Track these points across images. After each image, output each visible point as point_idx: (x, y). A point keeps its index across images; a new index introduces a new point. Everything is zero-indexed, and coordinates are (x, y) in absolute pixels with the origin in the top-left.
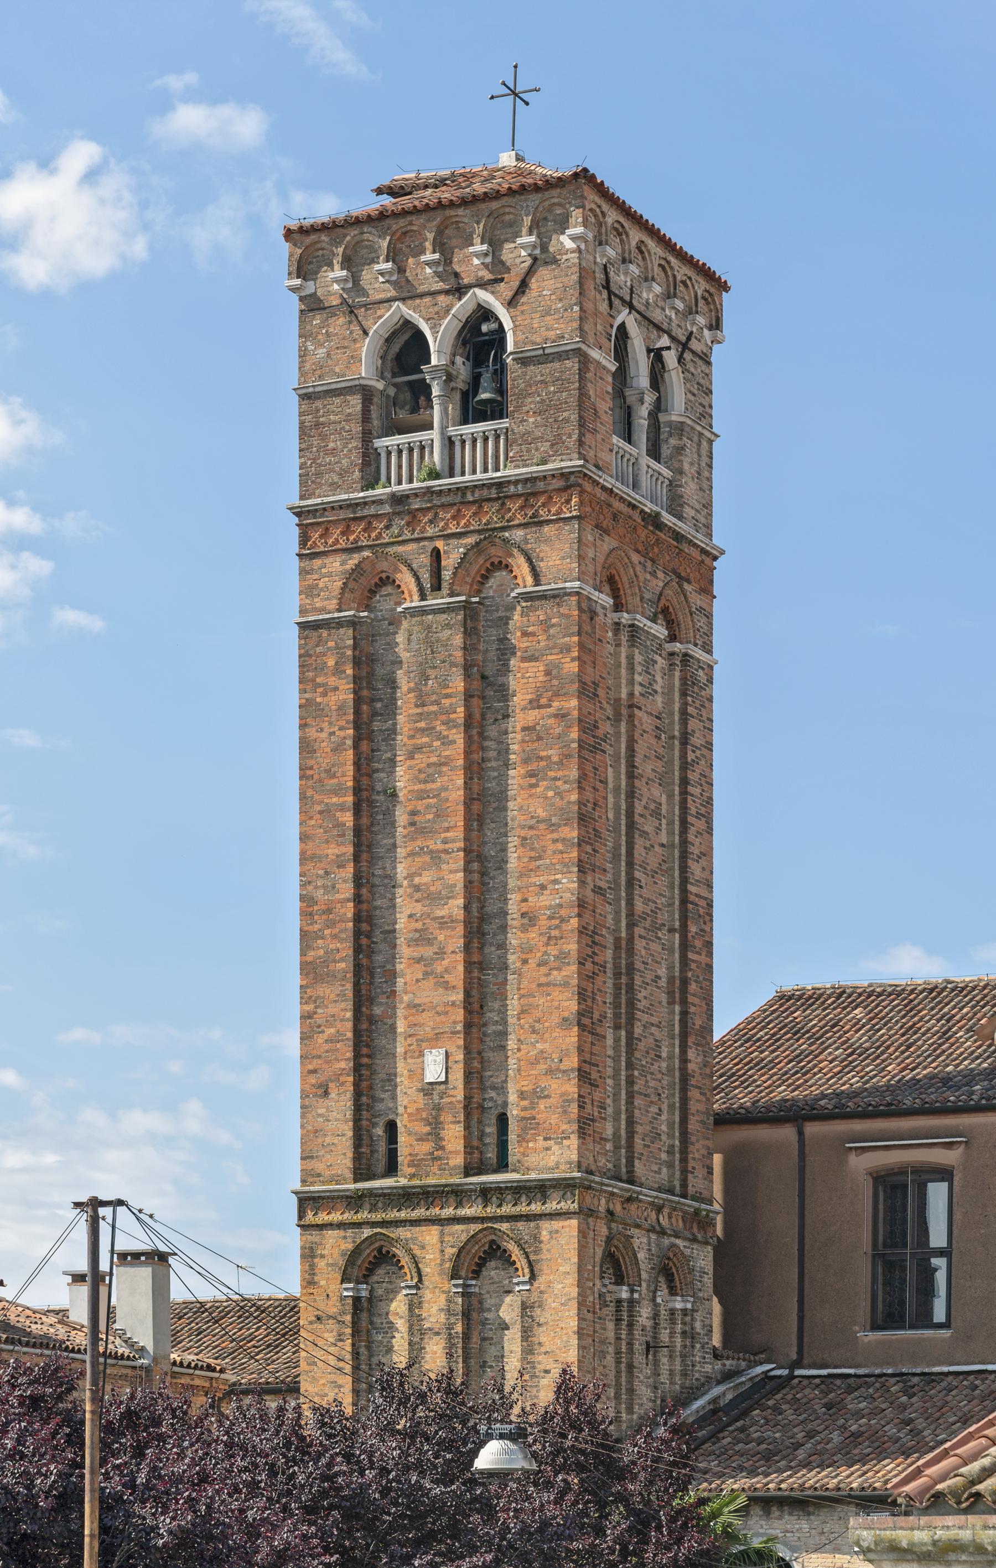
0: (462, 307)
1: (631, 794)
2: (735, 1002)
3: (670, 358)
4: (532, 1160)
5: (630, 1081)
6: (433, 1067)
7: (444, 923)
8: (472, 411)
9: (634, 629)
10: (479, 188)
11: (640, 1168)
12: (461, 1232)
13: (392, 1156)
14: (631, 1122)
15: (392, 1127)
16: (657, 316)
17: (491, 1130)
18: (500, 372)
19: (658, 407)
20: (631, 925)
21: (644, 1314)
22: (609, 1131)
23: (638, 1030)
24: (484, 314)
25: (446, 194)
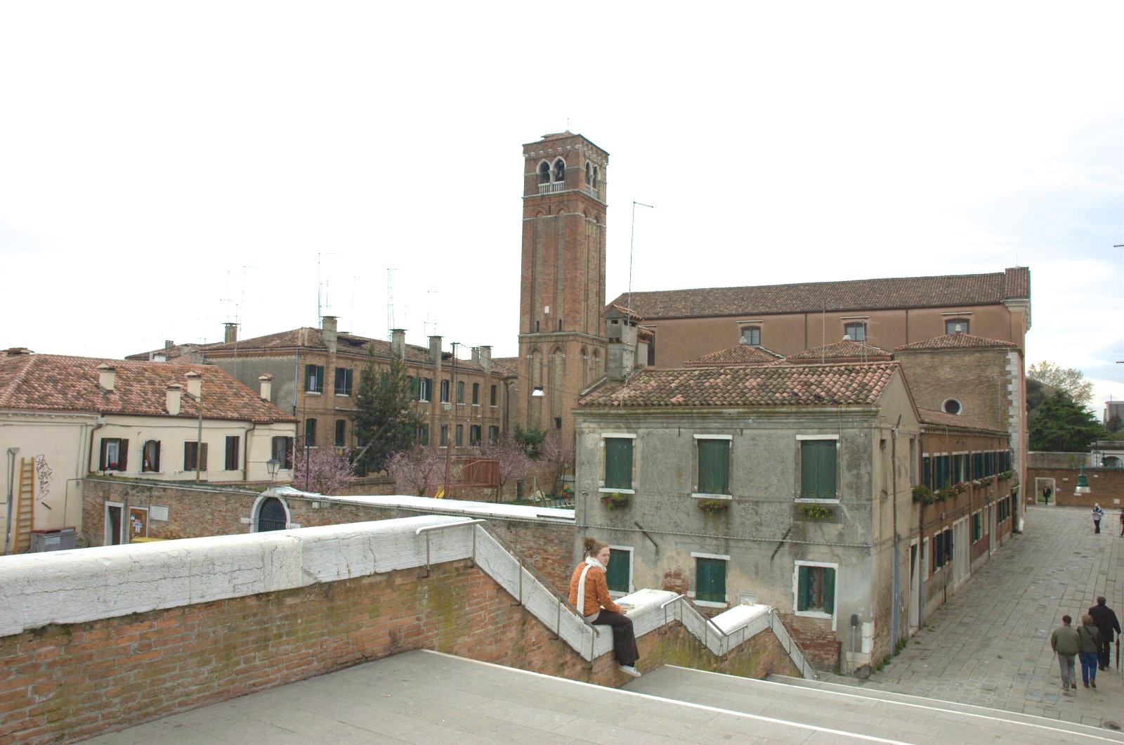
0: (556, 160)
1: (588, 254)
2: (611, 296)
3: (598, 168)
4: (565, 329)
5: (587, 313)
6: (547, 310)
7: (549, 280)
8: (558, 179)
9: (589, 221)
10: (560, 137)
11: (589, 331)
12: (552, 344)
13: (538, 328)
14: (587, 322)
15: (538, 323)
16: (595, 161)
17: (558, 323)
18: (563, 172)
19: (595, 177)
20: (588, 281)
21: (589, 362)
22: (582, 323)
23: (589, 302)
24: (560, 161)
25: (553, 138)
